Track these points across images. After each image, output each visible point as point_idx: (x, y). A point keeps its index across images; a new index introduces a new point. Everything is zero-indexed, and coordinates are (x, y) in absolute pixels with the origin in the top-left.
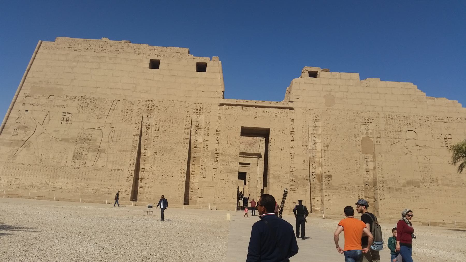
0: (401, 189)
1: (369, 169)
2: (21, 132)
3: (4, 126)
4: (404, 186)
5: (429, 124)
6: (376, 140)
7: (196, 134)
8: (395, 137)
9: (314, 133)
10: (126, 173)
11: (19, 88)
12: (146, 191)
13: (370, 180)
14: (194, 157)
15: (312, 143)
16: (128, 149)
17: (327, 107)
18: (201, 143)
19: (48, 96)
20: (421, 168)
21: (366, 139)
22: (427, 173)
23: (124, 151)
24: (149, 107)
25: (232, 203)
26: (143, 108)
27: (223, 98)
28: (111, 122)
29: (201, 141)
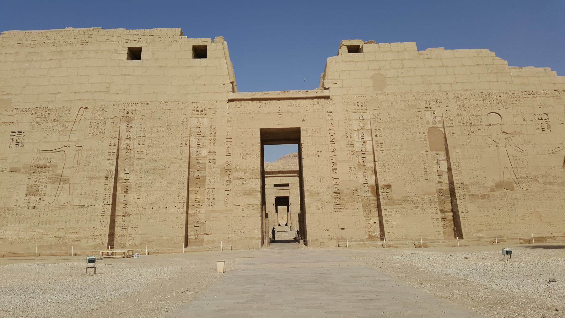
0: (488, 195)
1: (442, 172)
5: (518, 103)
7: (199, 145)
8: (473, 124)
14: (198, 178)
15: (360, 143)
16: (101, 175)
17: (376, 92)
18: (205, 157)
20: (513, 164)
22: (522, 169)
23: (95, 178)
26: (120, 115)
27: (233, 91)
29: (206, 154)
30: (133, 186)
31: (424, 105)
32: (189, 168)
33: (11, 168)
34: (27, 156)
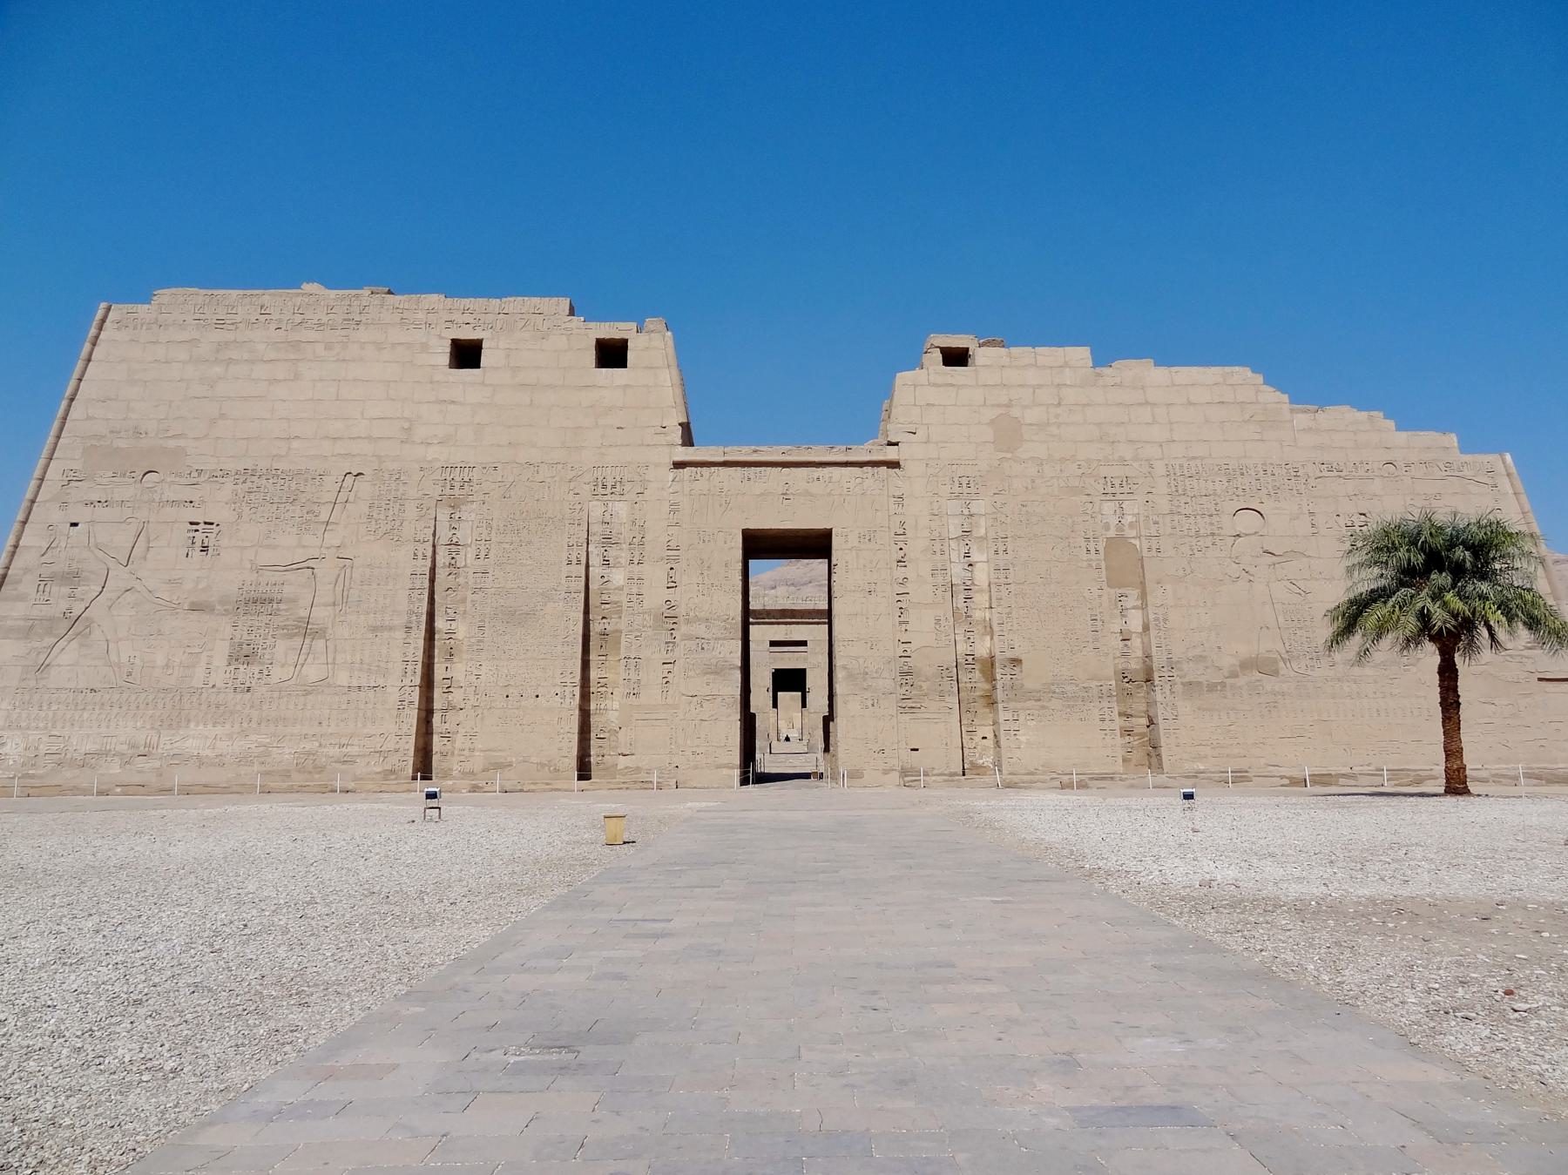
2: (59, 591)
6: (1145, 545)
10: (393, 696)
11: (45, 453)
12: (458, 745)
14: (604, 634)
15: (960, 567)
17: (1002, 455)
18: (621, 589)
20: (1281, 619)
21: (1117, 544)
23: (382, 628)
24: (455, 493)
25: (727, 766)
26: (436, 492)
28: (337, 542)
29: (622, 583)
30: (465, 648)
31: (1100, 488)
32: (587, 612)
33: (192, 603)
34: (228, 574)
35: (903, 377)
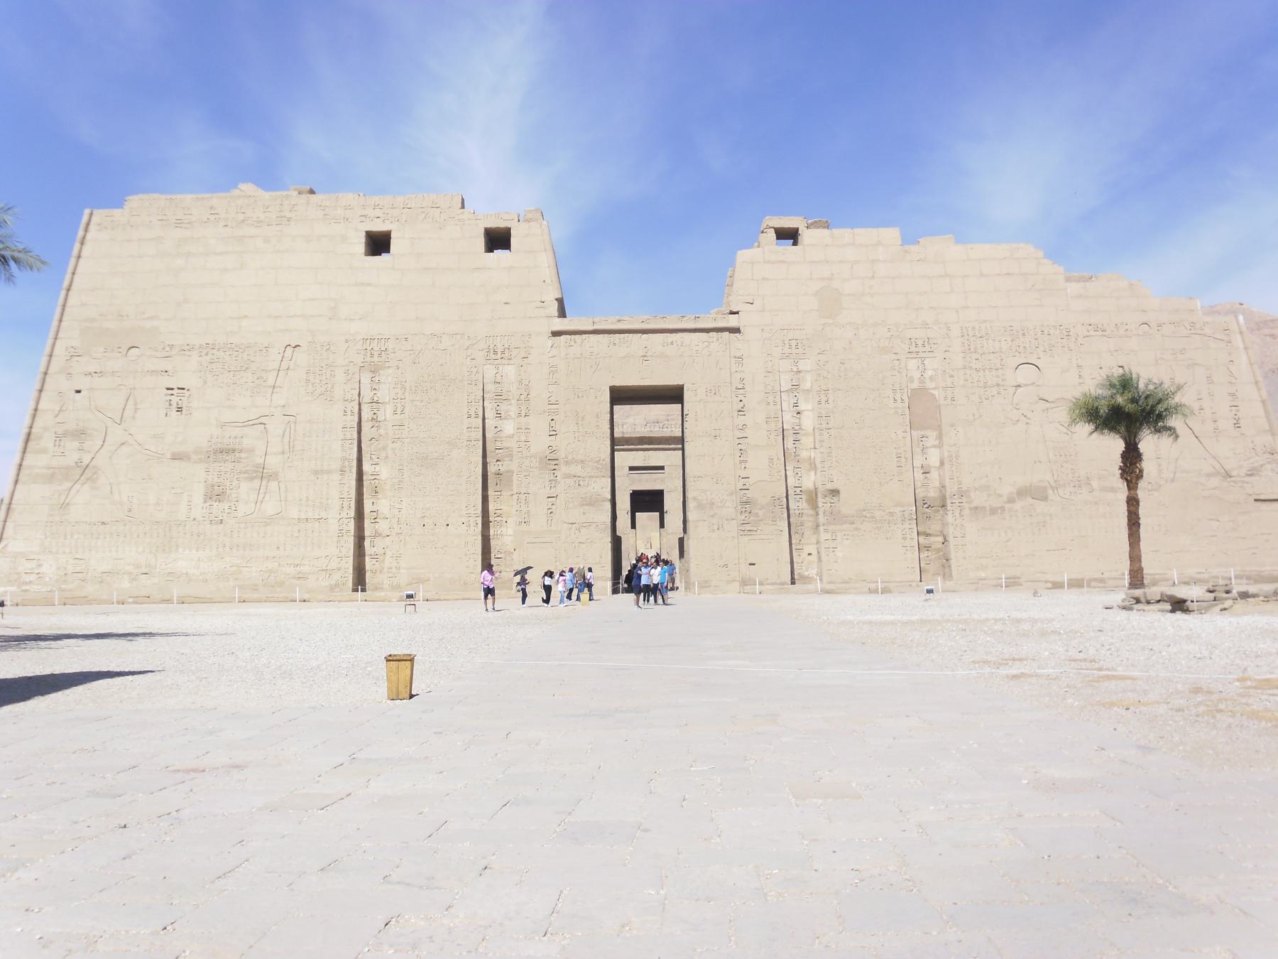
2: (72, 445)
3: (29, 434)
4: (1011, 500)
7: (499, 415)
9: (796, 387)
11: (52, 335)
12: (387, 564)
13: (933, 493)
18: (512, 436)
19: (124, 350)
28: (283, 403)
33: (173, 454)
35: (743, 255)
